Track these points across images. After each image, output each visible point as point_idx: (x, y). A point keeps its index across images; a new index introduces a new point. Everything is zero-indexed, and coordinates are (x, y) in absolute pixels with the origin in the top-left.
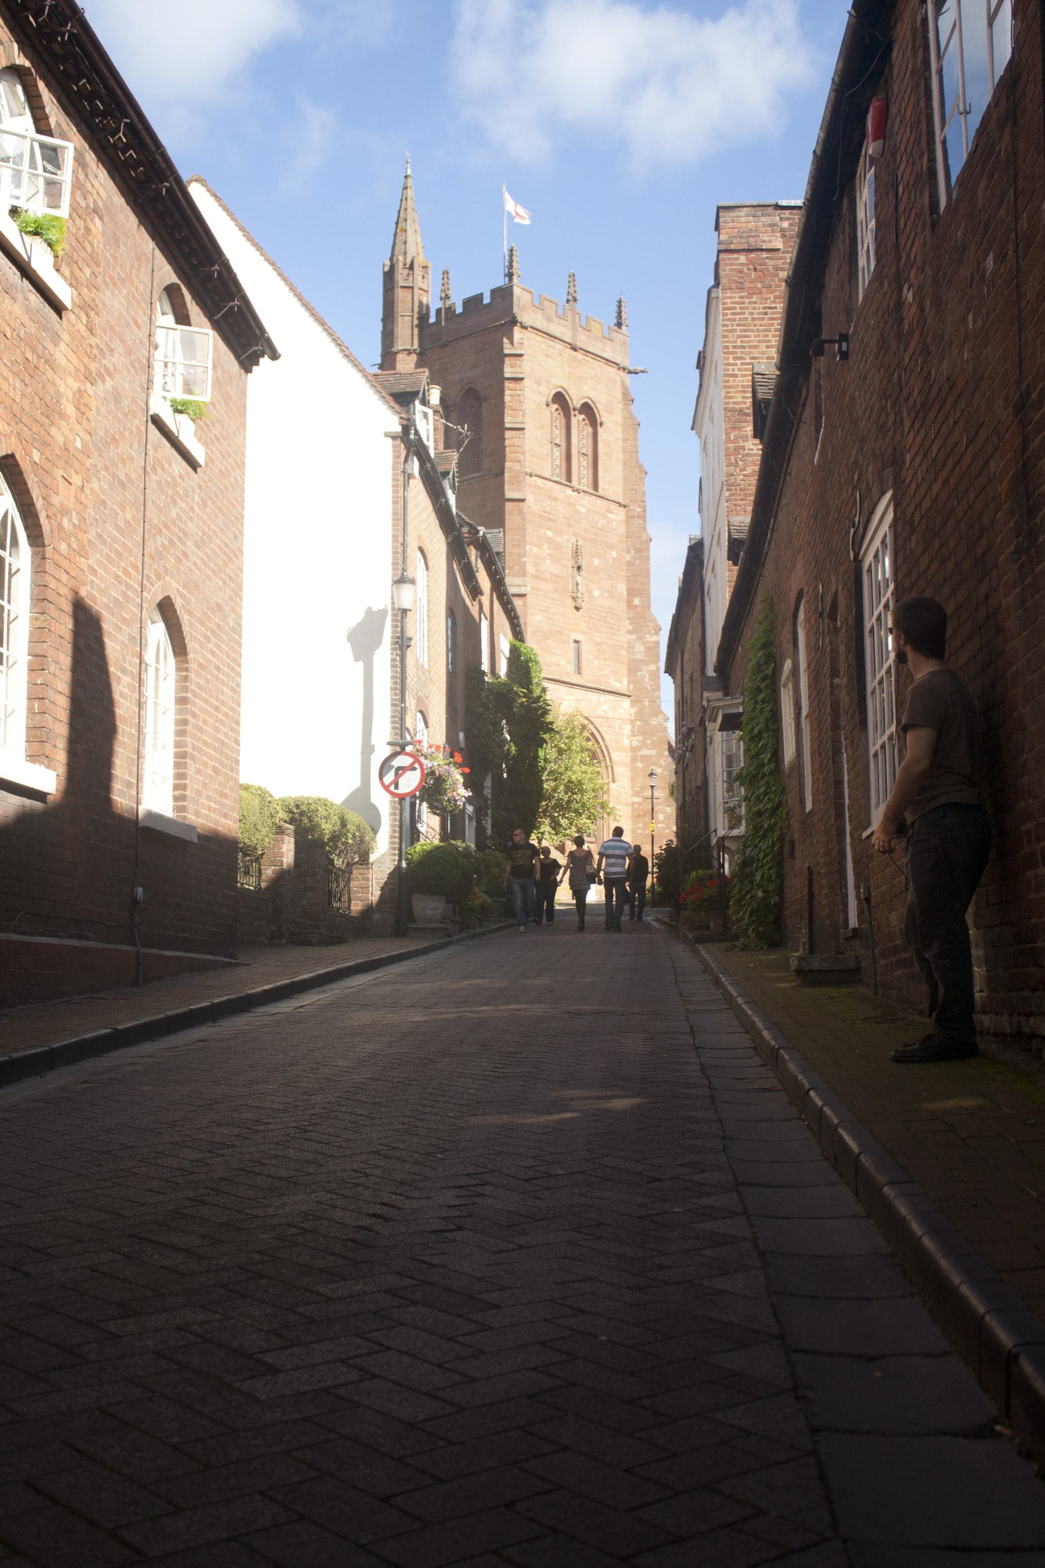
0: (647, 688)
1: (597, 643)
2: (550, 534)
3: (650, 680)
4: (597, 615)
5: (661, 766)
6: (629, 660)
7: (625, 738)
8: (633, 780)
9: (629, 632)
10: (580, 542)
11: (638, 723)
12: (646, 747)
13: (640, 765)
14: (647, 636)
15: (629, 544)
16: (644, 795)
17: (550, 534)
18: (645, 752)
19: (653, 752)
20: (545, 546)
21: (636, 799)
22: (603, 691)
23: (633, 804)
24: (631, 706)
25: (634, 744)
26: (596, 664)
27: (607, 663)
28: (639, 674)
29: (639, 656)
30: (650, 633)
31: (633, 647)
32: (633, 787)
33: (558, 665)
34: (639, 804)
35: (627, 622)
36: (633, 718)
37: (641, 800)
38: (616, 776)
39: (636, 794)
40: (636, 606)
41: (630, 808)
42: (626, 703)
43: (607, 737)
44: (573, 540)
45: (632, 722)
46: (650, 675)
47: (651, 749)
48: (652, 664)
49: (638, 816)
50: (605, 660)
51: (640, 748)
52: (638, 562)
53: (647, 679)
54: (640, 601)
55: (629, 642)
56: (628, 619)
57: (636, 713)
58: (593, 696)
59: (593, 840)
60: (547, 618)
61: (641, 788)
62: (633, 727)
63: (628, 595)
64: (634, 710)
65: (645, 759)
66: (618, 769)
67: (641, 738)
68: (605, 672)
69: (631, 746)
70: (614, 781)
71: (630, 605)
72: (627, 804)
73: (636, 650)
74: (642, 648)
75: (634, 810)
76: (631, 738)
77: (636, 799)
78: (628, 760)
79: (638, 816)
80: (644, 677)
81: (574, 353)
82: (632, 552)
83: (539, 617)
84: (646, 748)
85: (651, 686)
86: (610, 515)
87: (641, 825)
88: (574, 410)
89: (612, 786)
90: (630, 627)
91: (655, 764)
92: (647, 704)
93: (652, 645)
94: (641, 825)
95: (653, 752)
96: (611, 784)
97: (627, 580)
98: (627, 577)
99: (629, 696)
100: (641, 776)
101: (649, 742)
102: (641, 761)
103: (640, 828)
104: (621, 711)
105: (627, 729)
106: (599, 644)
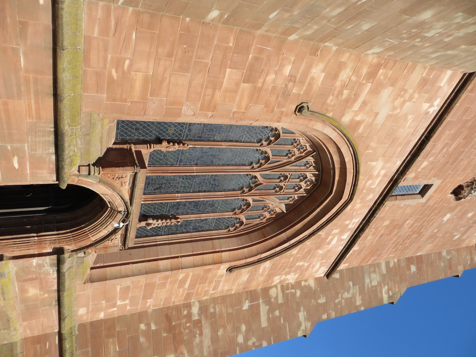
0: (338, 298)
3: (347, 299)
5: (246, 339)
6: (362, 267)
7: (283, 277)
8: (224, 299)
9: (387, 263)
11: (298, 293)
12: (271, 311)
13: (246, 306)
14: (386, 287)
15: (453, 252)
16: (203, 322)
18: (264, 309)
19: (264, 323)
21: (195, 310)
23: (188, 306)
24: (318, 280)
25: (273, 292)
28: (351, 283)
29: (367, 281)
30: (389, 290)
31: (374, 272)
32: (214, 300)
34: (189, 315)
35: (396, 260)
36: (303, 283)
37: (196, 318)
38: (235, 272)
39: (203, 309)
40: (409, 269)
41: (182, 302)
42: (322, 271)
43: (294, 251)
45: (297, 284)
46: (351, 298)
47: (268, 319)
48: (362, 300)
49: (168, 318)
51: (268, 301)
52: (442, 264)
53: (346, 295)
54: (414, 272)
55: (379, 265)
56: (398, 260)
57: (309, 287)
59: (130, 243)
61: (213, 315)
62: (293, 287)
63: (417, 257)
64: (312, 283)
65: (254, 311)
66: (245, 274)
67: (280, 301)
69: (271, 287)
70: (230, 270)
71: (410, 261)
72: (188, 296)
73: (373, 275)
74: (375, 283)
75: (178, 308)
76: (279, 286)
77: (195, 310)
78: (253, 286)
79: (168, 318)
80: (348, 292)
82: (449, 257)
84: (269, 312)
85: (340, 302)
87: (153, 327)
89: (223, 268)
90: (391, 265)
91: (248, 331)
92: (322, 300)
93: (379, 294)
94: (153, 327)
95: (264, 323)
96: (223, 268)
97: (428, 254)
98: (431, 254)
100: (230, 311)
101: (277, 313)
102: (251, 307)
103: (148, 325)
105: (291, 278)
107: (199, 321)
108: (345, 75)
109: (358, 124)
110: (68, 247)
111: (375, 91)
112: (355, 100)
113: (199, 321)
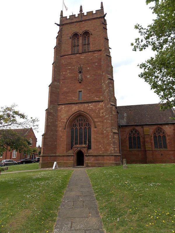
1: (88, 90)
2: (70, 67)
4: (89, 82)
10: (82, 65)
17: (70, 67)
20: (68, 71)
22: (90, 102)
26: (88, 95)
27: (93, 94)
29: (105, 89)
33: (72, 99)
42: (101, 104)
44: (79, 66)
50: (92, 93)
58: (86, 105)
60: (68, 88)
68: (92, 97)
81: (80, 23)
83: (65, 89)
86: (94, 55)
88: (81, 35)
99: (103, 101)
104: (99, 106)
106: (90, 90)
107: (107, 131)
108: (60, 125)
109: (66, 118)
110: (85, 155)
111: (62, 119)
112: (63, 121)
113: (107, 131)
